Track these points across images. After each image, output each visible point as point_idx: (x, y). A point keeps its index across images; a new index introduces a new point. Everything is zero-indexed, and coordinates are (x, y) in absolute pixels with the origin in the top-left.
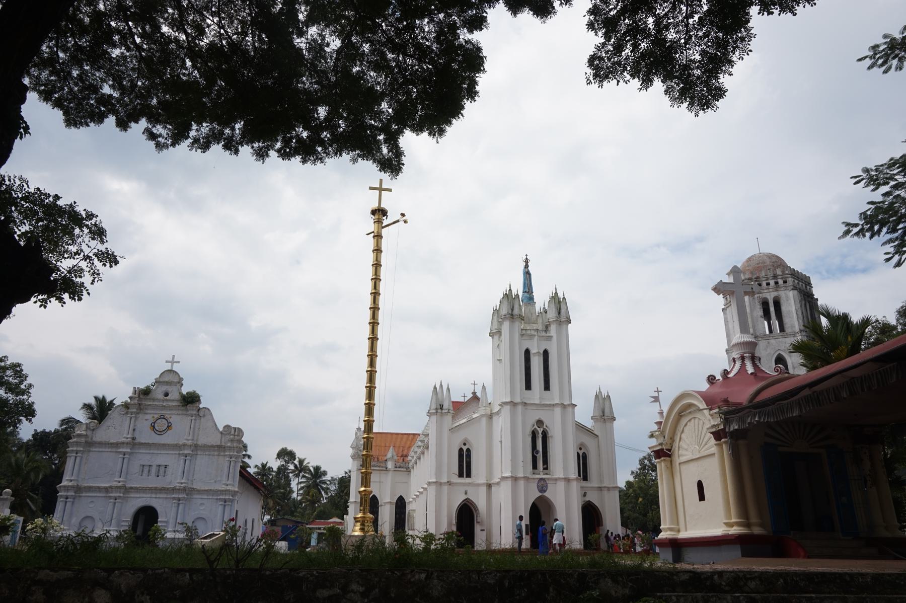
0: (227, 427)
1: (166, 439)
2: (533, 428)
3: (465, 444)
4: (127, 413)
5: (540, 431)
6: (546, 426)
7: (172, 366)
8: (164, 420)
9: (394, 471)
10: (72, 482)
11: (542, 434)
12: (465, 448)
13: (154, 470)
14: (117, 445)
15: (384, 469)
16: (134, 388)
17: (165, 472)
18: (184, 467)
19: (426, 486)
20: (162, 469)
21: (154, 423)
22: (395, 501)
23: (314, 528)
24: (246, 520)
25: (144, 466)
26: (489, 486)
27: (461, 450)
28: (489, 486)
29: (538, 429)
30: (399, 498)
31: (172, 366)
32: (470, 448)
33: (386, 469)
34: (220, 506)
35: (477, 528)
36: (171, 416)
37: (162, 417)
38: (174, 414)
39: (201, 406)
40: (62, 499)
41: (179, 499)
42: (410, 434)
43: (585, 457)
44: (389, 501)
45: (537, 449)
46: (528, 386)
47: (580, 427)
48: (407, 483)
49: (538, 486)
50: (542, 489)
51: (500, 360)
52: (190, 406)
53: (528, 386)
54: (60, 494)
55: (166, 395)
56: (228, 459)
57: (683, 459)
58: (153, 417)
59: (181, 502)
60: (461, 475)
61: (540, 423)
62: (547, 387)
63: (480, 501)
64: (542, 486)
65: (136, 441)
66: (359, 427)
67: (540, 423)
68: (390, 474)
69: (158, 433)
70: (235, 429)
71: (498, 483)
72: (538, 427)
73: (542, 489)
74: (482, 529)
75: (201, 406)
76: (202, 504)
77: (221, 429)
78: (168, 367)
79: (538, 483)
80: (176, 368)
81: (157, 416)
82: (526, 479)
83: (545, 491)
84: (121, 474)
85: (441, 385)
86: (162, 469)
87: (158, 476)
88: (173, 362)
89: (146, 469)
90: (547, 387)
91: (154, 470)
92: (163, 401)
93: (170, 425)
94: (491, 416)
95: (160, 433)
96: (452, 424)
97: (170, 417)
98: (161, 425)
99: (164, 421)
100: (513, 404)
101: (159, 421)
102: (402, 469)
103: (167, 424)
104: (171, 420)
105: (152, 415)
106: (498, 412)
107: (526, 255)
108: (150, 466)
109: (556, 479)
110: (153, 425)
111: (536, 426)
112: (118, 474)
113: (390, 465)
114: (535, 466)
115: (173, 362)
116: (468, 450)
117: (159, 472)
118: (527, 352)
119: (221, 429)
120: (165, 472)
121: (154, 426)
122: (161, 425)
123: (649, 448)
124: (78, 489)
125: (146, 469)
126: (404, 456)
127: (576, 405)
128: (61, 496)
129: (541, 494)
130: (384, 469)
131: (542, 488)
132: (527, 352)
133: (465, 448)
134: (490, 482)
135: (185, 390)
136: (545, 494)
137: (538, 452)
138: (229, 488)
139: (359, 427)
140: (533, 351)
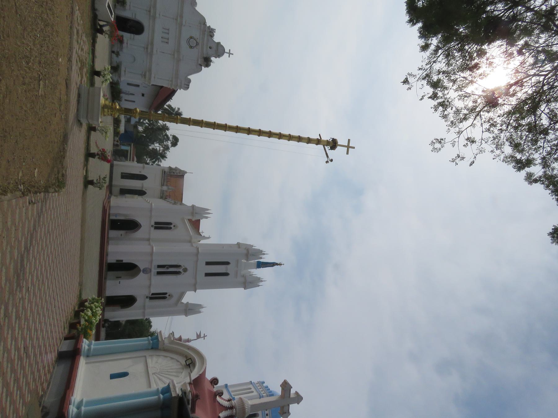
0: (189, 81)
2: (182, 266)
3: (174, 226)
5: (181, 270)
6: (183, 274)
7: (227, 53)
11: (179, 271)
12: (172, 226)
13: (165, 36)
14: (182, 17)
15: (163, 184)
16: (215, 30)
19: (150, 202)
20: (166, 41)
21: (194, 39)
23: (131, 147)
24: (133, 95)
26: (148, 240)
27: (171, 224)
28: (148, 240)
29: (182, 269)
30: (145, 192)
31: (227, 53)
32: (172, 229)
35: (122, 232)
36: (198, 48)
37: (197, 44)
39: (203, 67)
43: (164, 298)
45: (170, 268)
46: (208, 263)
47: (182, 295)
49: (147, 268)
51: (223, 247)
53: (208, 263)
55: (210, 48)
56: (170, 79)
57: (149, 361)
60: (156, 223)
61: (185, 270)
62: (207, 275)
63: (139, 234)
64: (147, 271)
66: (187, 173)
67: (185, 270)
70: (189, 85)
71: (150, 244)
72: (183, 269)
74: (122, 235)
75: (203, 67)
78: (227, 50)
79: (149, 268)
80: (226, 55)
81: (198, 41)
82: (151, 261)
83: (143, 272)
85: (209, 213)
86: (166, 41)
89: (167, 31)
90: (207, 275)
91: (165, 36)
93: (193, 48)
94: (190, 242)
95: (188, 42)
96: (186, 219)
97: (197, 49)
99: (195, 45)
100: (197, 253)
101: (195, 42)
103: (193, 46)
106: (192, 246)
107: (284, 264)
108: (169, 34)
109: (150, 279)
110: (193, 38)
111: (183, 267)
113: (165, 188)
114: (159, 266)
115: (230, 53)
116: (170, 228)
117: (164, 38)
118: (227, 263)
119: (189, 77)
121: (192, 38)
122: (193, 43)
123: (160, 332)
125: (167, 31)
126: (170, 197)
127: (195, 292)
129: (142, 270)
130: (163, 184)
131: (146, 271)
132: (227, 263)
133: (172, 226)
134: (151, 240)
135: (213, 59)
136: (141, 272)
137: (168, 268)
138: (152, 79)
139: (187, 173)
140: (229, 266)
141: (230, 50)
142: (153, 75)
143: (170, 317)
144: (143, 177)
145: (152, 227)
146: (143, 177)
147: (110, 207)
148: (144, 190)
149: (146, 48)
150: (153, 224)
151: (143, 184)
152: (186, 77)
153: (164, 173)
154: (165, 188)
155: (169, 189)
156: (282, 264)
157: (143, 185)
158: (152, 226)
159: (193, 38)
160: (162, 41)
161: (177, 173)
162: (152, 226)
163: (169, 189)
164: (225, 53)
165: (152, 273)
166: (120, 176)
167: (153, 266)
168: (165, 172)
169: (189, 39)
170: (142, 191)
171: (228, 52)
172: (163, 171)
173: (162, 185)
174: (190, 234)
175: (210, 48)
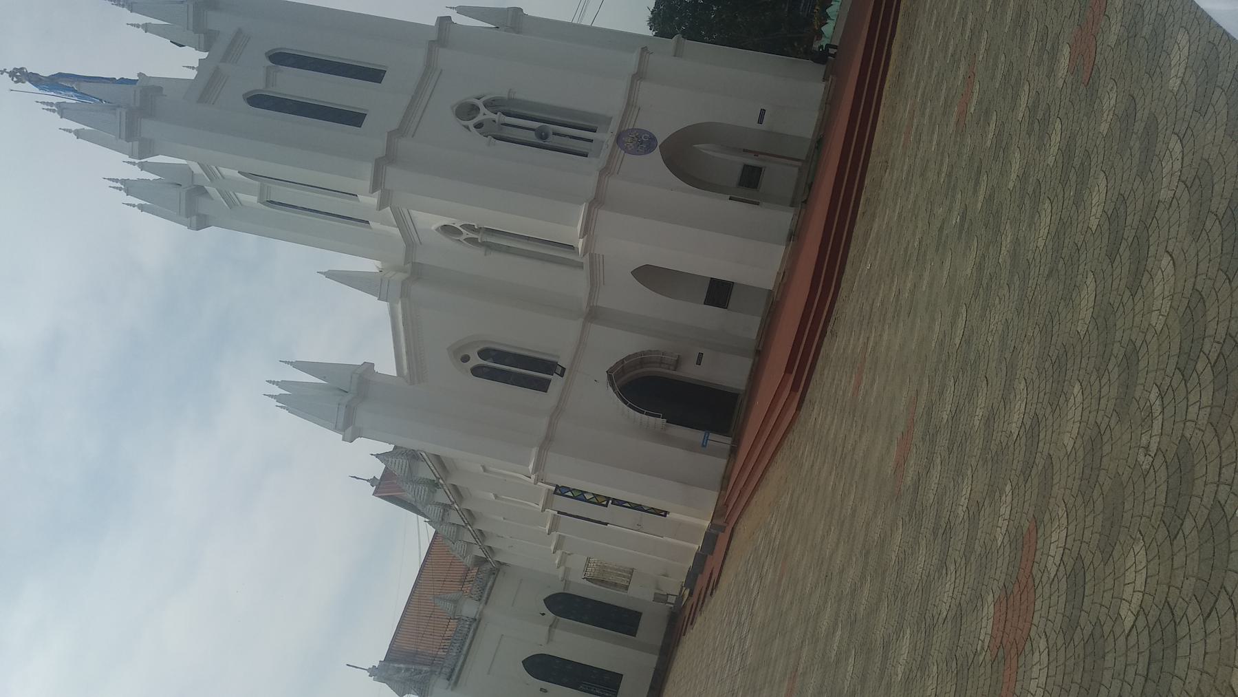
9: (486, 603)
12: (476, 361)
15: (474, 625)
27: (477, 372)
33: (476, 621)
35: (691, 372)
46: (354, 119)
50: (644, 143)
53: (354, 119)
60: (543, 386)
62: (374, 75)
63: (623, 345)
66: (368, 670)
73: (644, 143)
90: (374, 75)
102: (490, 584)
113: (469, 609)
130: (474, 625)
139: (368, 670)
143: (586, 22)
145: (564, 369)
147: (723, 487)
150: (556, 382)
151: (549, 640)
153: (453, 670)
154: (469, 609)
155: (455, 602)
156: (12, 74)
157: (549, 631)
158: (562, 375)
161: (407, 670)
162: (562, 375)
163: (455, 602)
165: (614, 127)
167: (605, 154)
168: (449, 679)
172: (456, 683)
173: (476, 621)
174: (403, 309)
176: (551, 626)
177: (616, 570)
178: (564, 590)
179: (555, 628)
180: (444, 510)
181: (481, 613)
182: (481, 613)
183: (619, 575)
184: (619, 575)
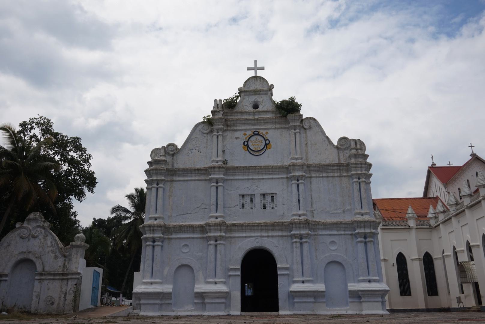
0: (343, 140)
1: (266, 160)
4: (211, 132)
7: (256, 73)
8: (259, 137)
10: (158, 221)
13: (258, 200)
14: (206, 171)
15: (407, 227)
16: (216, 101)
17: (273, 202)
18: (299, 195)
20: (268, 199)
21: (248, 142)
22: (422, 258)
25: (243, 196)
31: (256, 73)
34: (359, 244)
37: (256, 133)
38: (271, 129)
40: (148, 243)
41: (301, 237)
42: (411, 198)
44: (418, 257)
48: (431, 239)
52: (290, 116)
54: (145, 236)
55: (256, 106)
56: (355, 180)
58: (245, 134)
59: (304, 240)
65: (228, 166)
68: (414, 231)
69: (254, 153)
76: (333, 242)
77: (335, 143)
78: (252, 74)
80: (260, 73)
81: (249, 133)
84: (217, 207)
86: (268, 199)
87: (264, 208)
88: (256, 69)
89: (247, 200)
91: (258, 200)
92: (254, 113)
93: (267, 142)
95: (256, 153)
97: (267, 133)
98: (257, 143)
101: (253, 138)
103: (264, 141)
104: (268, 137)
105: (243, 132)
110: (246, 143)
112: (213, 207)
113: (412, 223)
115: (256, 69)
117: (264, 203)
119: (335, 143)
120: (273, 202)
121: (248, 146)
122: (257, 143)
124: (167, 229)
125: (247, 200)
128: (146, 239)
138: (367, 218)
141: (249, 69)
142: (359, 218)
144: (401, 260)
146: (401, 260)
148: (422, 257)
149: (301, 239)
151: (413, 260)
152: (337, 148)
153: (387, 226)
159: (246, 143)
160: (273, 208)
164: (258, 75)
166: (407, 298)
169: (251, 152)
170: (424, 259)
171: (258, 66)
175: (256, 106)
176: (419, 258)
177: (472, 275)
178: (435, 258)
179: (419, 260)
180: (468, 195)
181: (412, 228)
182: (412, 228)
183: (471, 277)
184: (471, 277)
